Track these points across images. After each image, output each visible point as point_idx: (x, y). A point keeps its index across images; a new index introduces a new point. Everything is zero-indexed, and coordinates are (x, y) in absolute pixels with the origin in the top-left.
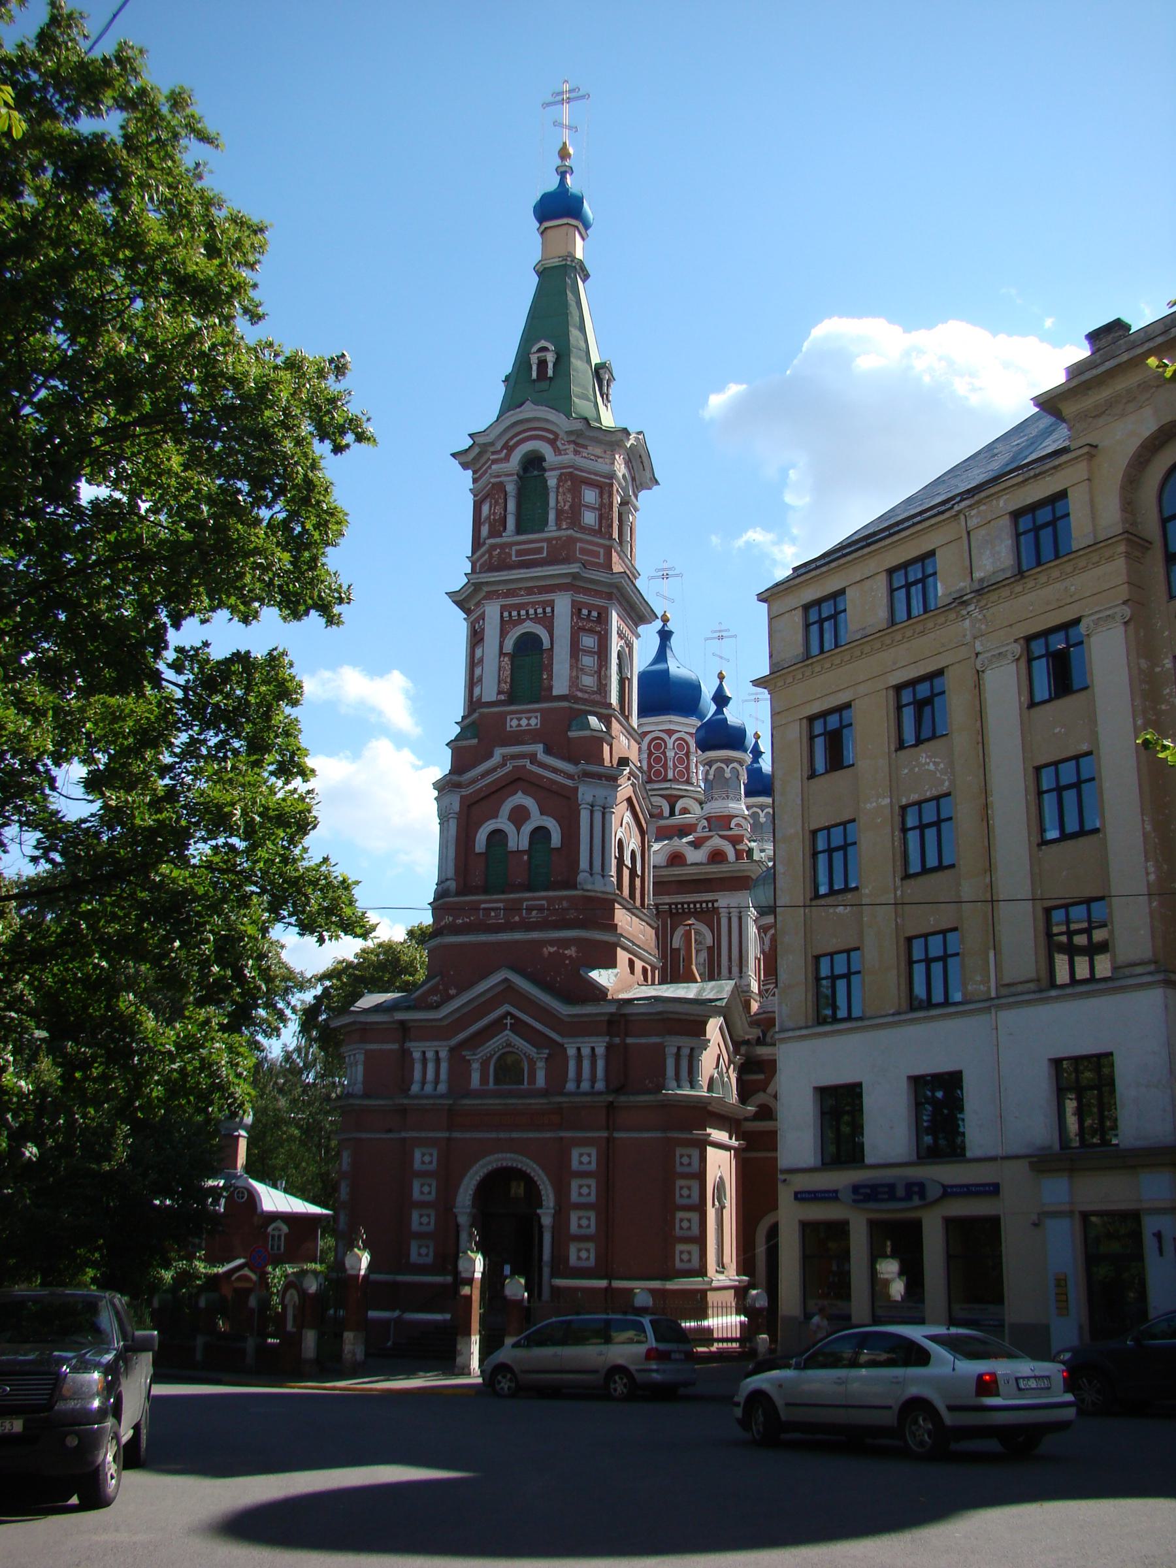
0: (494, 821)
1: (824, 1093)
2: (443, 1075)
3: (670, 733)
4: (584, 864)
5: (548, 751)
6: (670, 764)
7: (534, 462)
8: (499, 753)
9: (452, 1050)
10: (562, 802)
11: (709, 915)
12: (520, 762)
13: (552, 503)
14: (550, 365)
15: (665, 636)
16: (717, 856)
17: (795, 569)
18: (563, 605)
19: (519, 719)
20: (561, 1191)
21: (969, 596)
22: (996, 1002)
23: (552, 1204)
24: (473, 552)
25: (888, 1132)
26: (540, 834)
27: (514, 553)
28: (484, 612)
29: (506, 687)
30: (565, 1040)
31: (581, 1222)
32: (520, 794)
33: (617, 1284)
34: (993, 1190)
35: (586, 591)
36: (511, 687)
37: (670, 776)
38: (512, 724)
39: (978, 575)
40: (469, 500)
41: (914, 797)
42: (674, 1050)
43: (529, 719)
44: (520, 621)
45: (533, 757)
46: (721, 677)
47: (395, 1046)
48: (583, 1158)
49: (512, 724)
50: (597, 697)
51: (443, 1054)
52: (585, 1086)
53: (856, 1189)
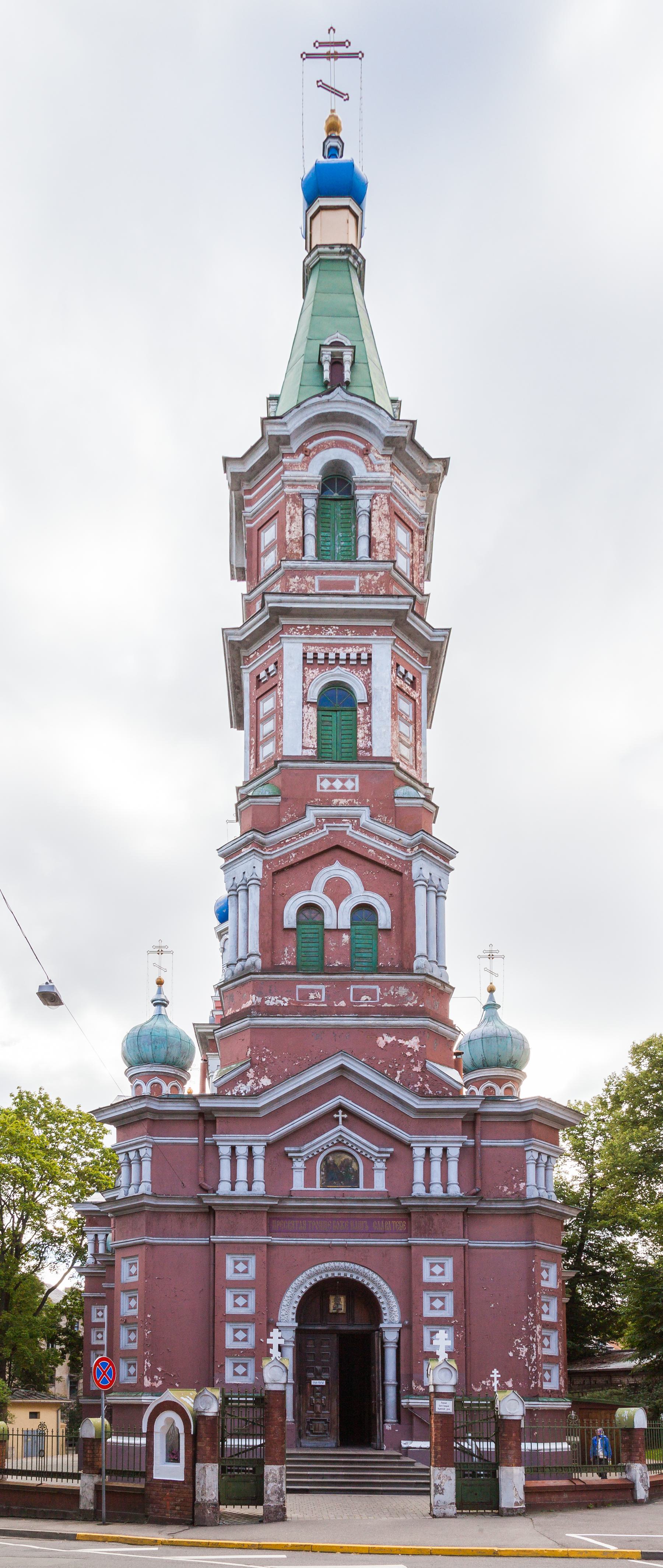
0: (307, 893)
4: (420, 948)
7: (337, 480)
8: (312, 814)
9: (269, 1146)
12: (338, 827)
14: (347, 367)
19: (332, 780)
23: (397, 1319)
26: (364, 910)
27: (317, 584)
28: (280, 653)
30: (415, 1138)
32: (337, 865)
38: (323, 785)
43: (344, 781)
47: (195, 1140)
48: (438, 1270)
49: (323, 785)
51: (259, 1150)
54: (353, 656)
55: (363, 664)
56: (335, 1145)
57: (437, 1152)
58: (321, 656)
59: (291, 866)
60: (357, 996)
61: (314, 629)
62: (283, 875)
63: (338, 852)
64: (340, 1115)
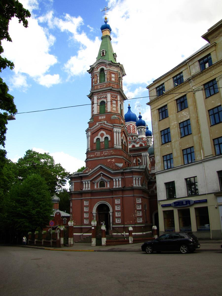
1: (166, 184)
2: (89, 186)
3: (131, 125)
4: (115, 143)
5: (107, 123)
6: (131, 130)
7: (102, 70)
9: (91, 181)
10: (110, 132)
11: (140, 156)
13: (106, 77)
14: (105, 53)
15: (129, 108)
16: (141, 145)
17: (153, 82)
19: (101, 117)
20: (114, 208)
21: (191, 78)
22: (204, 160)
23: (112, 211)
24: (92, 88)
25: (181, 191)
26: (106, 138)
29: (99, 111)
31: (117, 215)
32: (102, 131)
33: (125, 226)
34: (206, 201)
35: (113, 92)
36: (100, 111)
37: (132, 132)
38: (100, 118)
39: (192, 74)
40: (91, 79)
41: (182, 121)
42: (135, 178)
43: (103, 117)
44: (101, 98)
45: (104, 123)
46: (140, 113)
47: (80, 181)
49: (100, 118)
50: (116, 112)
52: (117, 187)
53: (175, 203)
54: (104, 97)
55: (106, 98)
56: (101, 180)
57: (117, 180)
58: (100, 97)
59: (95, 132)
60: (105, 153)
61: (98, 94)
62: (94, 134)
63: (102, 129)
64: (102, 175)
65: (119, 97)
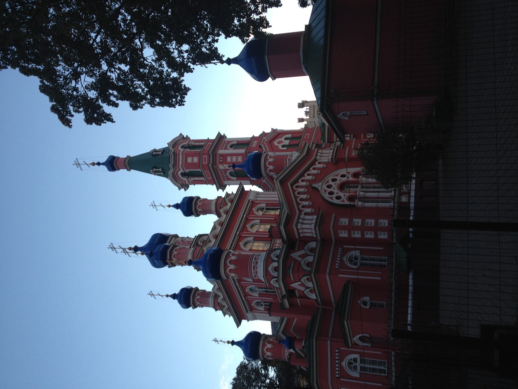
7: (184, 174)
18: (221, 167)
35: (216, 161)
44: (227, 176)
65: (221, 152)
